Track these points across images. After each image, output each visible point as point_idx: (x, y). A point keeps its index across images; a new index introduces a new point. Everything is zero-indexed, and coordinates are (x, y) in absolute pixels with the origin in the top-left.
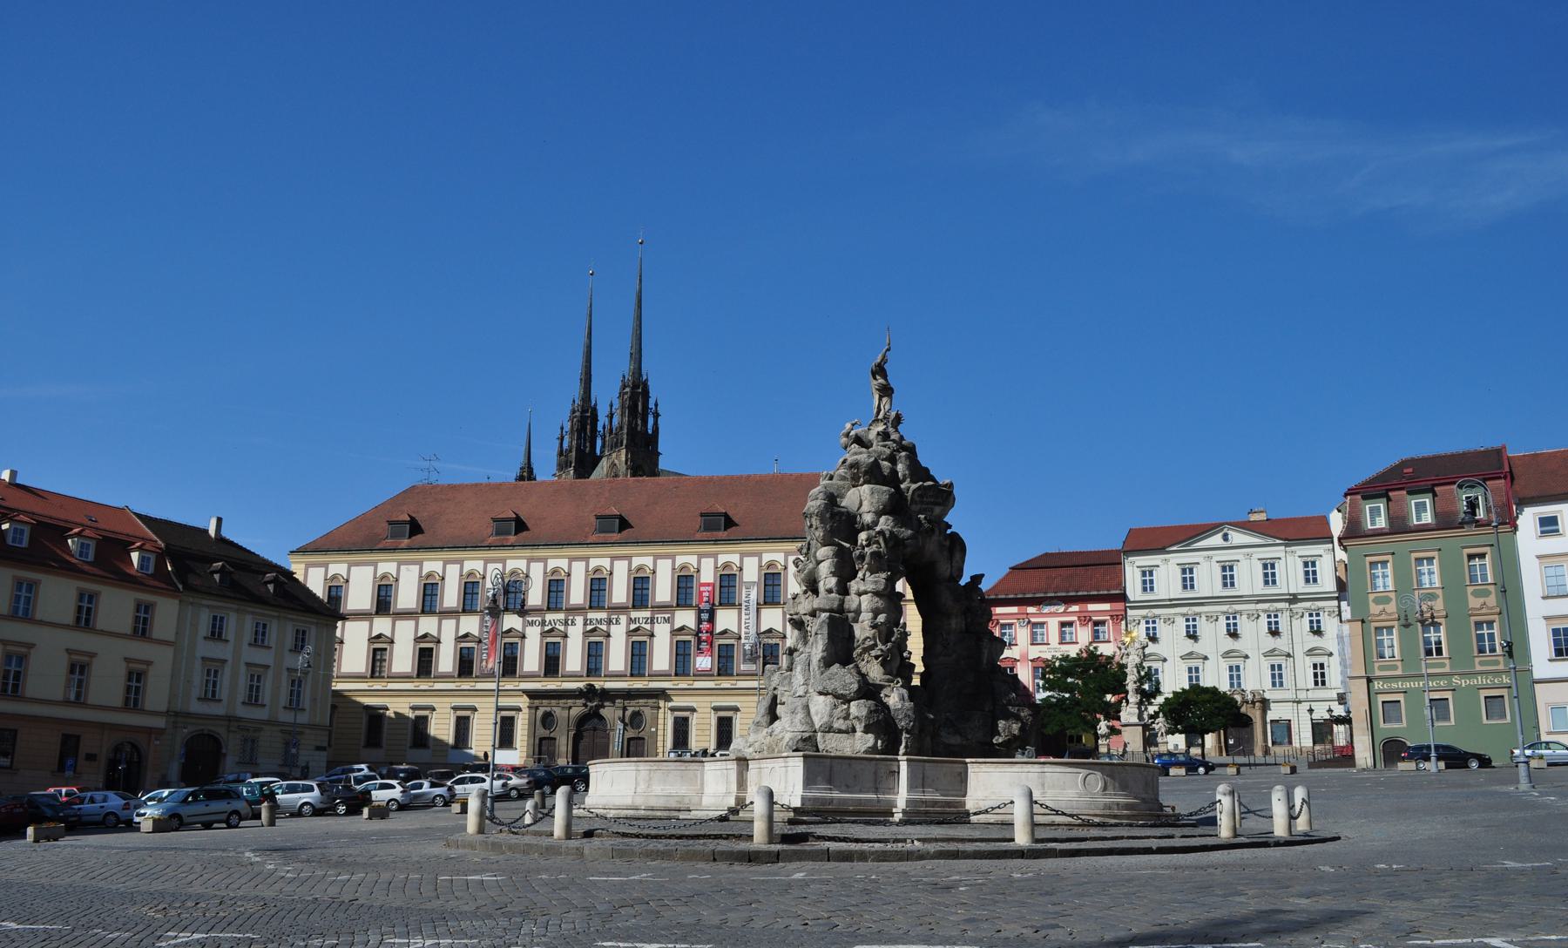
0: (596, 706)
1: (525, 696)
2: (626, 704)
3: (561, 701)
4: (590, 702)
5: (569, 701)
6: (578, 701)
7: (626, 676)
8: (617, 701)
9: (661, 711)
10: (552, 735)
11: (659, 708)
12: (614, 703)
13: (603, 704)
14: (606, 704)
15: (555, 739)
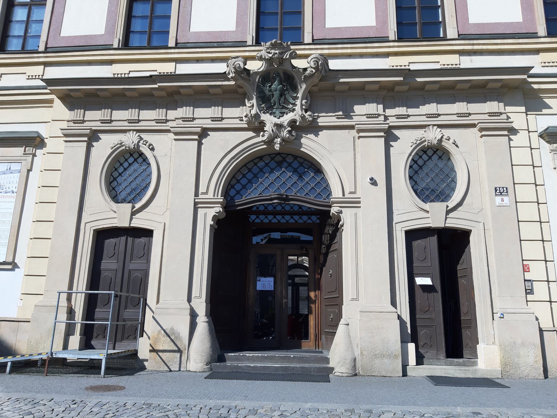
0: (292, 123)
1: (58, 102)
2: (393, 121)
3: (172, 114)
4: (269, 109)
5: (201, 112)
6: (228, 112)
7: (385, 39)
8: (359, 109)
9: (519, 139)
10: (139, 222)
11: (513, 131)
12: (348, 115)
13: (315, 120)
14: (324, 120)
15: (148, 233)
